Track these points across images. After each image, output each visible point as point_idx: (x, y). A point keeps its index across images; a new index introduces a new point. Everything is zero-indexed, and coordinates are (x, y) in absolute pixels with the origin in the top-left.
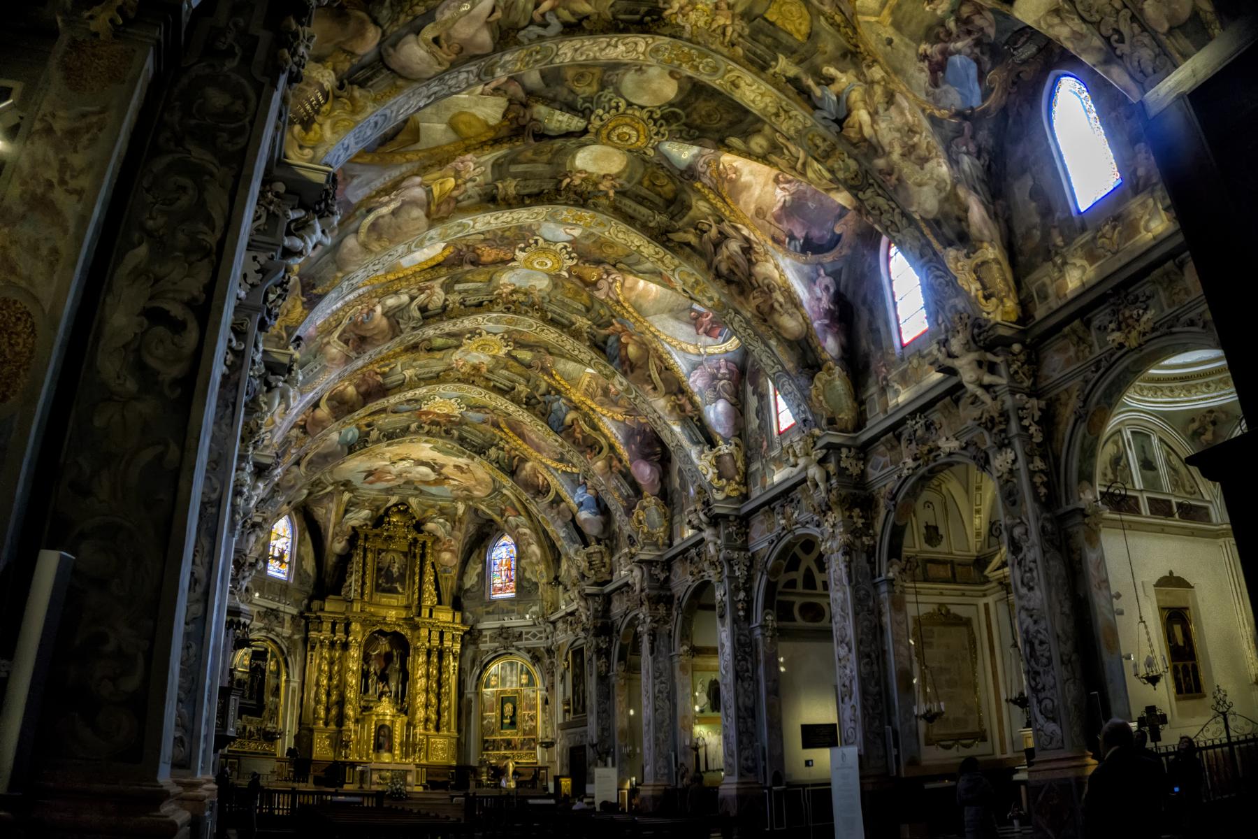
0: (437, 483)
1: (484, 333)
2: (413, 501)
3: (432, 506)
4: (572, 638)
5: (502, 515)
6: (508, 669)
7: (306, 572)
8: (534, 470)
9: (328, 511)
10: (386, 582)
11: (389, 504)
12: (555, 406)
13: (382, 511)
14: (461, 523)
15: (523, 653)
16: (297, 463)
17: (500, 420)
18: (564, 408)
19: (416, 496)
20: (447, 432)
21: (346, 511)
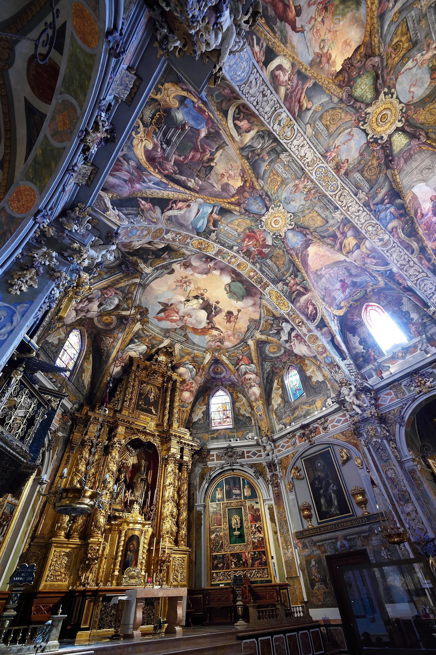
0: (204, 331)
1: (395, 96)
2: (178, 347)
3: (189, 354)
4: (301, 450)
5: (237, 364)
6: (232, 483)
7: (83, 382)
8: (309, 302)
9: (116, 340)
10: (144, 405)
11: (162, 346)
12: (382, 215)
13: (154, 350)
14: (203, 370)
15: (246, 469)
16: (163, 204)
17: (300, 255)
18: (389, 217)
19: (182, 343)
20: (254, 264)
21: (132, 341)
